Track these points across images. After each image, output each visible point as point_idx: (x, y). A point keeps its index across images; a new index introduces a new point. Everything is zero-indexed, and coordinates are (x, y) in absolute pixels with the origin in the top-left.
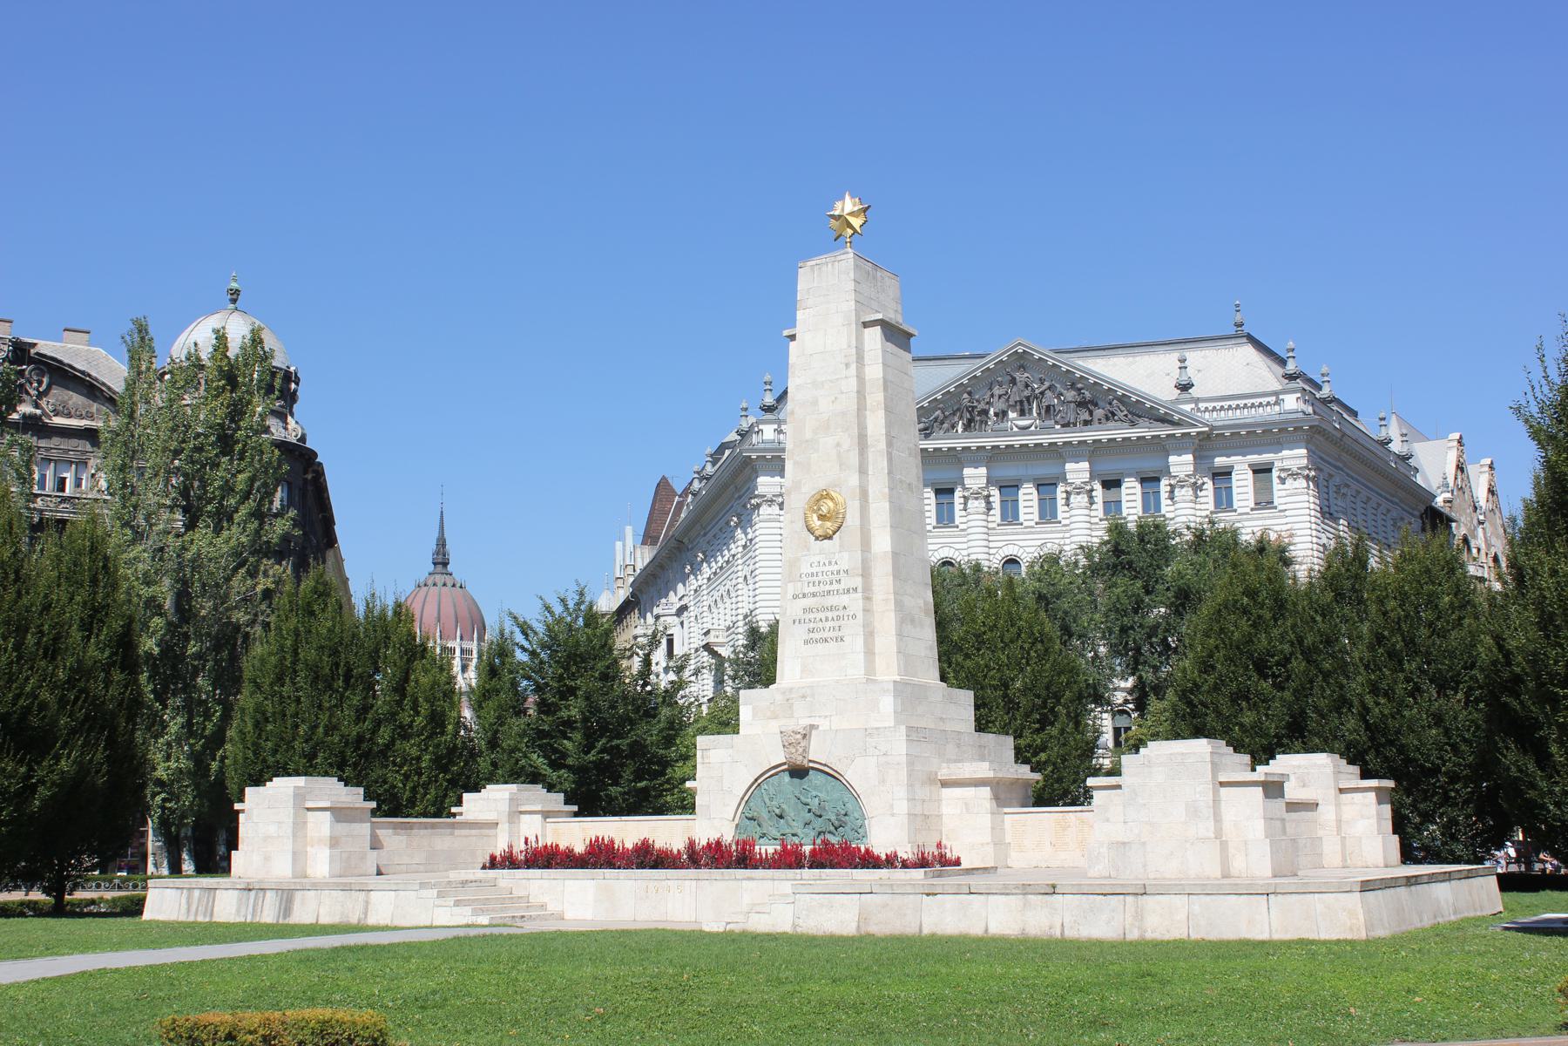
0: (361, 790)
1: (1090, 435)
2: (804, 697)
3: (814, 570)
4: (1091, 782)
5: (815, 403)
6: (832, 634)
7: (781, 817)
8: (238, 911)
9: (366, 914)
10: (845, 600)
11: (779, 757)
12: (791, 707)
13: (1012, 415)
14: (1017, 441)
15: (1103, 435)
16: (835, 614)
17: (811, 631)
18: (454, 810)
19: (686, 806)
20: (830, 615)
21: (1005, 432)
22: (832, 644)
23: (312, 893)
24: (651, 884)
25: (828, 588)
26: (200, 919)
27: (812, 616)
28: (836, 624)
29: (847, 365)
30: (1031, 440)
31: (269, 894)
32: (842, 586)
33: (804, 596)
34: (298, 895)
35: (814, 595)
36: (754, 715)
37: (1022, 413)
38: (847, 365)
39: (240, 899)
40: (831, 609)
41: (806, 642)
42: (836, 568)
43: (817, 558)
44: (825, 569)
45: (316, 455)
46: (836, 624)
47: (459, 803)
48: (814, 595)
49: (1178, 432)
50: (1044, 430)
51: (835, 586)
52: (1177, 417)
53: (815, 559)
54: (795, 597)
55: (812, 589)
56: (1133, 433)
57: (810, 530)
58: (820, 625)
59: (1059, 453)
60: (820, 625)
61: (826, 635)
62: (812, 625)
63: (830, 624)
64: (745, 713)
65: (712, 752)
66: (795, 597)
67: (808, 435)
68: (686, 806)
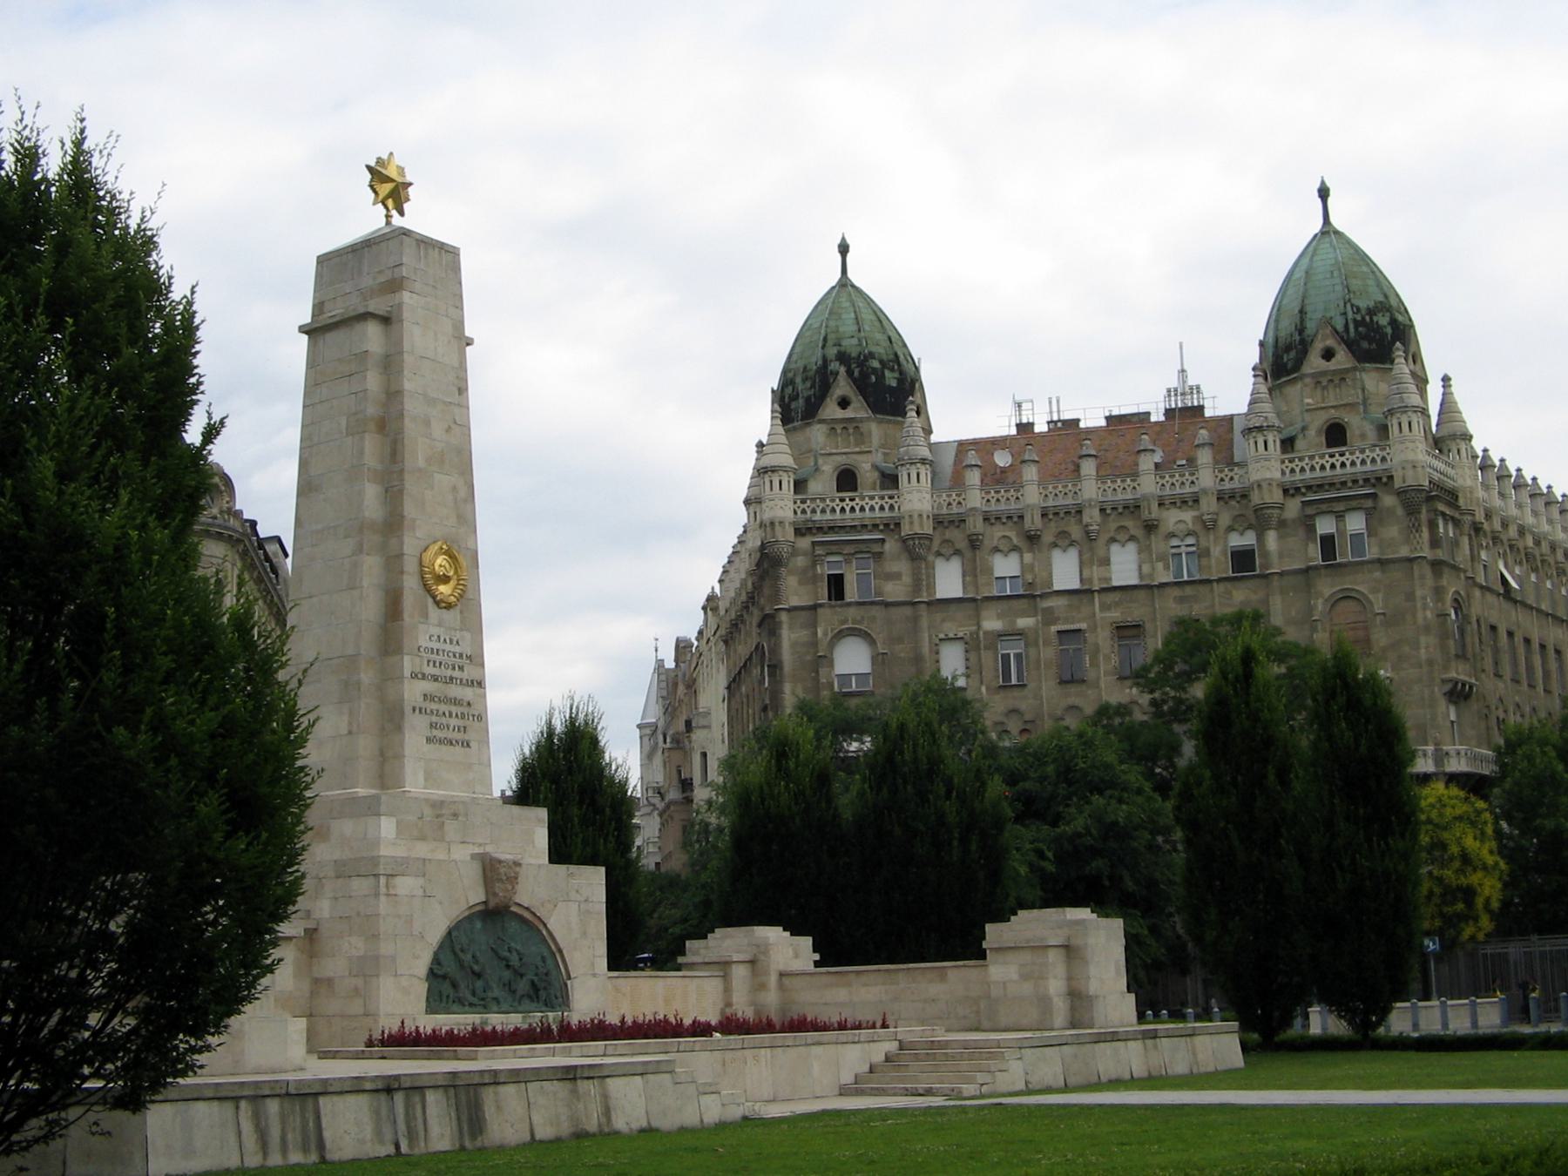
2: (455, 815)
3: (435, 645)
5: (427, 423)
7: (478, 975)
8: (378, 1133)
9: (609, 1119)
11: (477, 896)
16: (459, 710)
17: (433, 726)
20: (454, 709)
22: (458, 749)
23: (510, 1090)
24: (729, 1055)
25: (449, 673)
26: (296, 1157)
27: (434, 706)
28: (460, 722)
31: (431, 1097)
32: (465, 675)
33: (424, 677)
34: (488, 1095)
36: (399, 832)
39: (377, 1112)
40: (456, 702)
41: (429, 740)
42: (457, 649)
43: (435, 631)
44: (448, 647)
46: (460, 722)
51: (457, 674)
53: (435, 631)
54: (414, 676)
57: (428, 590)
58: (444, 721)
60: (444, 721)
62: (434, 719)
63: (453, 722)
65: (399, 880)
67: (421, 463)
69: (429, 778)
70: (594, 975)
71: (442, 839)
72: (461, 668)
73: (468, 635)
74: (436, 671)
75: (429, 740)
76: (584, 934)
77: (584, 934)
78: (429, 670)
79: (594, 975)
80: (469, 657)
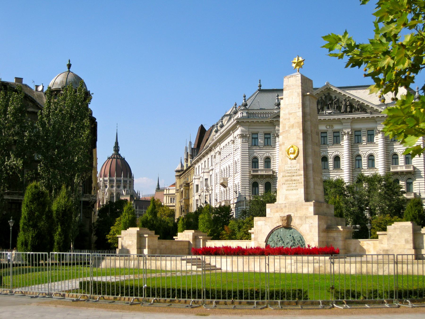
0: (154, 232)
1: (351, 116)
4: (378, 233)
5: (289, 119)
6: (294, 188)
10: (298, 178)
12: (282, 209)
13: (325, 108)
14: (327, 118)
15: (356, 116)
16: (295, 182)
18: (174, 237)
19: (247, 236)
20: (294, 182)
21: (323, 115)
22: (294, 192)
25: (293, 174)
27: (288, 182)
29: (299, 108)
30: (332, 117)
35: (289, 176)
36: (271, 211)
37: (328, 108)
38: (299, 108)
41: (286, 190)
42: (295, 168)
45: (96, 119)
47: (176, 236)
48: (289, 176)
49: (380, 116)
50: (335, 114)
52: (380, 110)
53: (290, 165)
54: (283, 177)
55: (288, 174)
56: (366, 116)
59: (339, 121)
61: (292, 188)
64: (268, 211)
66: (283, 177)
67: (287, 129)
68: (247, 236)
69: (286, 198)
70: (314, 241)
71: (282, 212)
72: (296, 173)
73: (298, 165)
74: (290, 174)
75: (286, 190)
76: (311, 231)
77: (311, 231)
78: (287, 175)
79: (314, 241)
80: (299, 170)
